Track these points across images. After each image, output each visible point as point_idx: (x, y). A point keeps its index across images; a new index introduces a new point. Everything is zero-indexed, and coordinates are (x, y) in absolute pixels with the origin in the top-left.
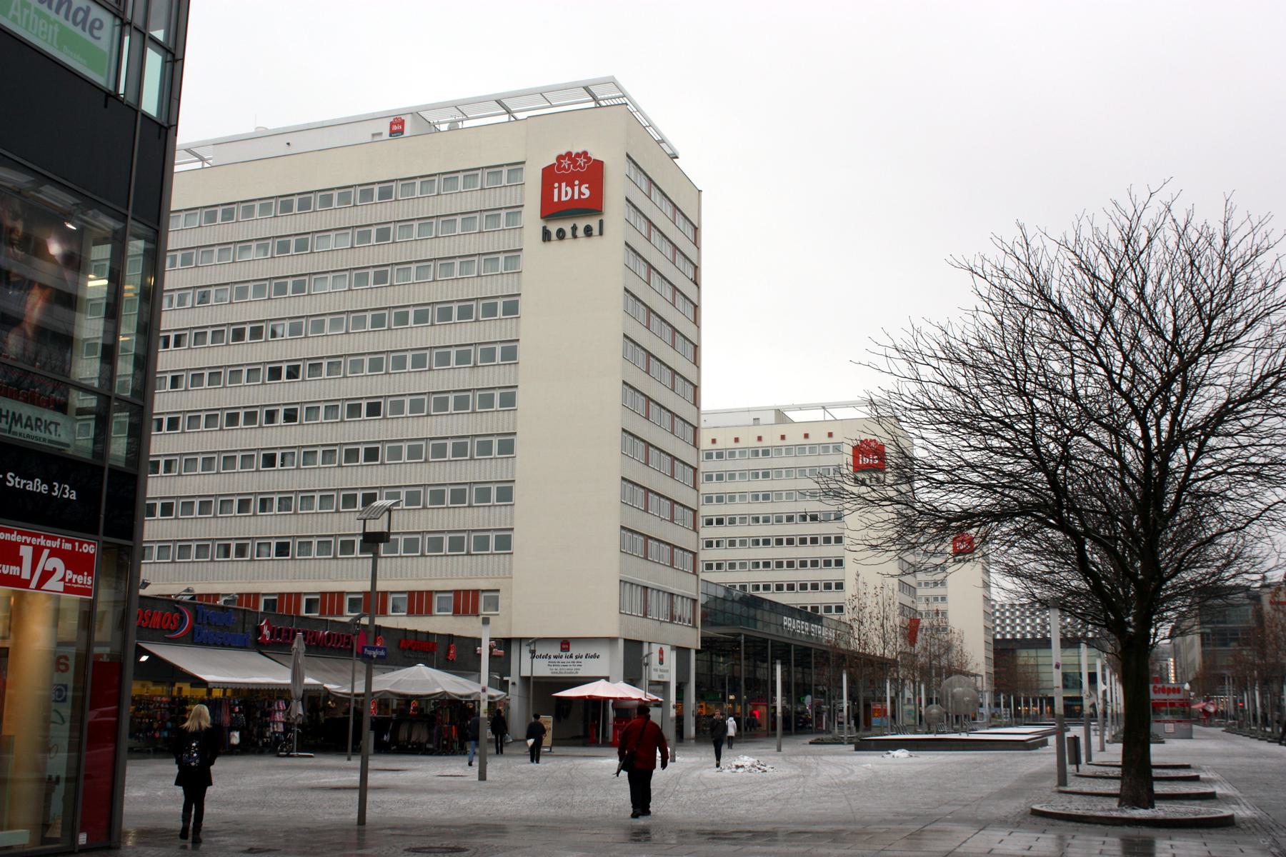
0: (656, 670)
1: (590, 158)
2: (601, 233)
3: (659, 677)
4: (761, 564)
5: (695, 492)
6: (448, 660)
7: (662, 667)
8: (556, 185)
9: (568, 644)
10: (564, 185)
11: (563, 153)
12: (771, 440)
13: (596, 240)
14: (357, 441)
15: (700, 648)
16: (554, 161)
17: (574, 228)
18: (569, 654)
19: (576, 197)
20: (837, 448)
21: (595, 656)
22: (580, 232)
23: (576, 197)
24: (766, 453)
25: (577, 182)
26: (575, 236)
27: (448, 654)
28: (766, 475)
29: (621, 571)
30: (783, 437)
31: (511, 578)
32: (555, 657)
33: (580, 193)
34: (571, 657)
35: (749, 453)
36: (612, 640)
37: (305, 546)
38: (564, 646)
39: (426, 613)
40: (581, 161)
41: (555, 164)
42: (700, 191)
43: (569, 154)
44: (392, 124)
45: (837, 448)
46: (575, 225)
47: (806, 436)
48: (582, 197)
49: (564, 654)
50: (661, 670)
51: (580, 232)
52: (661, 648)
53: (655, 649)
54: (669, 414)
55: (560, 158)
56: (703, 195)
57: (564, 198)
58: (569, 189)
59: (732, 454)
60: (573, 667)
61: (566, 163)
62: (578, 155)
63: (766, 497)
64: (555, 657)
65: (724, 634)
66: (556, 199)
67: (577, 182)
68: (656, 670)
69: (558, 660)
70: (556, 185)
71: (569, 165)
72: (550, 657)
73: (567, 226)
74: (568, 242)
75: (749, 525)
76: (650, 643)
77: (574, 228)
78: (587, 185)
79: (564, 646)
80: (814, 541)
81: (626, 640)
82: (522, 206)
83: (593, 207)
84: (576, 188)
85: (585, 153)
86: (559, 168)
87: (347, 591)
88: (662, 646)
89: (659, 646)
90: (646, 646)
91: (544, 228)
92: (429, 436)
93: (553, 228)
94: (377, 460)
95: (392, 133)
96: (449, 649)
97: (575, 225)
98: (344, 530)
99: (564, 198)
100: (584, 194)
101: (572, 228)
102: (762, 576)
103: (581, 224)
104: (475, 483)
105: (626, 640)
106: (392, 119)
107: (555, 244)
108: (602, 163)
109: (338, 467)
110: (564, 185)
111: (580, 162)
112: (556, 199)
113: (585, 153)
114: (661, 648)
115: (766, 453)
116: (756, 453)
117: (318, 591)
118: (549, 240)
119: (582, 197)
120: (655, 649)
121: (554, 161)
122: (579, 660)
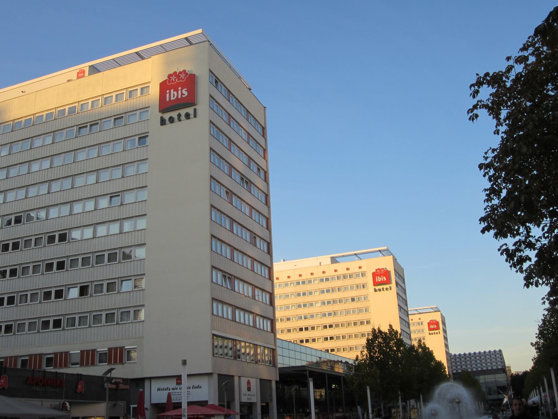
0: (245, 395)
1: (187, 74)
2: (195, 116)
3: (248, 399)
5: (270, 282)
6: (77, 392)
7: (249, 393)
8: (168, 91)
10: (172, 91)
11: (172, 73)
12: (330, 273)
13: (192, 120)
14: (52, 258)
15: (278, 380)
17: (179, 115)
19: (180, 97)
21: (199, 387)
23: (180, 97)
24: (327, 280)
25: (180, 88)
26: (180, 120)
27: (76, 388)
29: (213, 328)
30: (336, 271)
32: (173, 389)
36: (210, 374)
37: (21, 327)
38: (178, 381)
39: (91, 365)
41: (167, 79)
42: (265, 107)
43: (175, 73)
44: (78, 73)
46: (179, 113)
49: (178, 387)
50: (249, 395)
51: (183, 117)
52: (249, 380)
53: (244, 381)
54: (249, 232)
56: (267, 109)
57: (172, 98)
58: (175, 93)
59: (310, 282)
61: (173, 78)
62: (180, 73)
64: (173, 389)
65: (296, 371)
66: (168, 99)
67: (180, 88)
68: (245, 395)
69: (175, 391)
70: (168, 91)
71: (175, 79)
72: (170, 390)
73: (174, 114)
74: (176, 124)
76: (239, 377)
77: (179, 115)
78: (186, 89)
79: (178, 381)
81: (219, 375)
83: (190, 101)
84: (180, 92)
85: (184, 71)
86: (169, 82)
87: (45, 353)
88: (249, 379)
89: (246, 379)
90: (236, 379)
91: (162, 118)
92: (94, 251)
93: (167, 116)
94: (64, 269)
95: (78, 78)
96: (77, 385)
97: (179, 113)
98: (44, 314)
99: (172, 98)
100: (184, 95)
101: (178, 115)
102: (329, 345)
103: (183, 112)
104: (121, 277)
105: (219, 375)
106: (78, 71)
107: (169, 126)
108: (194, 75)
109: (41, 275)
110: (172, 91)
111: (181, 76)
112: (168, 99)
113: (184, 71)
114: (249, 380)
115: (327, 280)
116: (322, 280)
117: (28, 354)
118: (165, 124)
120: (244, 381)
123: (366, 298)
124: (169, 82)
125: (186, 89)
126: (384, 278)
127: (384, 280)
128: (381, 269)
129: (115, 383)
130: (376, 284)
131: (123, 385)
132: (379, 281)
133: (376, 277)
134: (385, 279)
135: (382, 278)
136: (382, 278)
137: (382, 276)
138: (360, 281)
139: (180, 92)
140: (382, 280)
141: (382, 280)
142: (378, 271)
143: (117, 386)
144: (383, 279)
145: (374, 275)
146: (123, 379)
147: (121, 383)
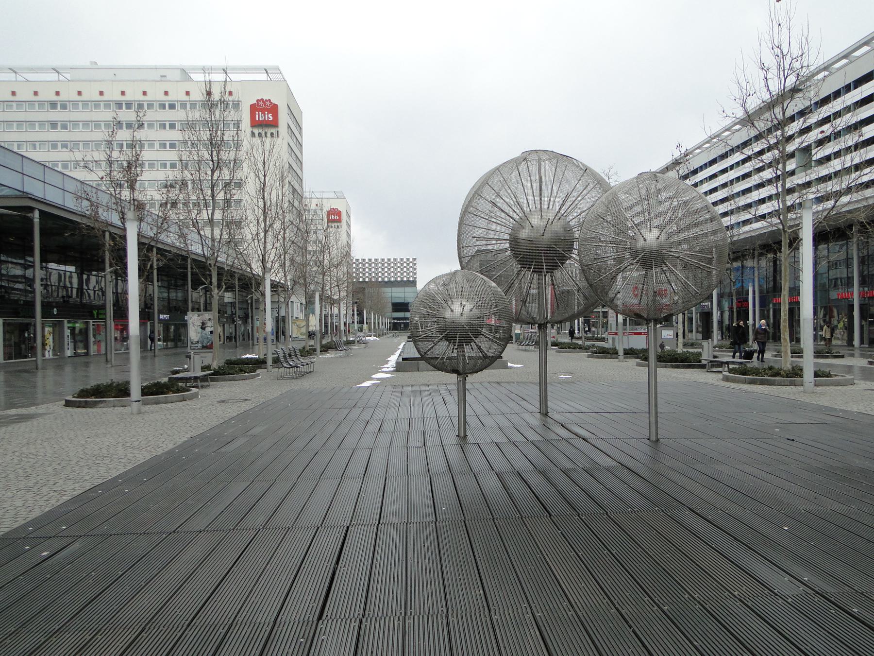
1: (272, 103)
16: (255, 102)
17: (266, 133)
22: (269, 135)
40: (268, 103)
43: (262, 99)
51: (269, 135)
55: (258, 101)
57: (261, 119)
61: (261, 103)
62: (266, 100)
66: (257, 119)
83: (274, 124)
84: (266, 115)
86: (258, 105)
91: (252, 132)
93: (256, 131)
99: (261, 119)
110: (260, 113)
113: (270, 100)
124: (258, 105)
126: (270, 115)
133: (257, 113)
135: (266, 115)
137: (266, 113)
140: (267, 119)
141: (267, 119)
145: (254, 108)
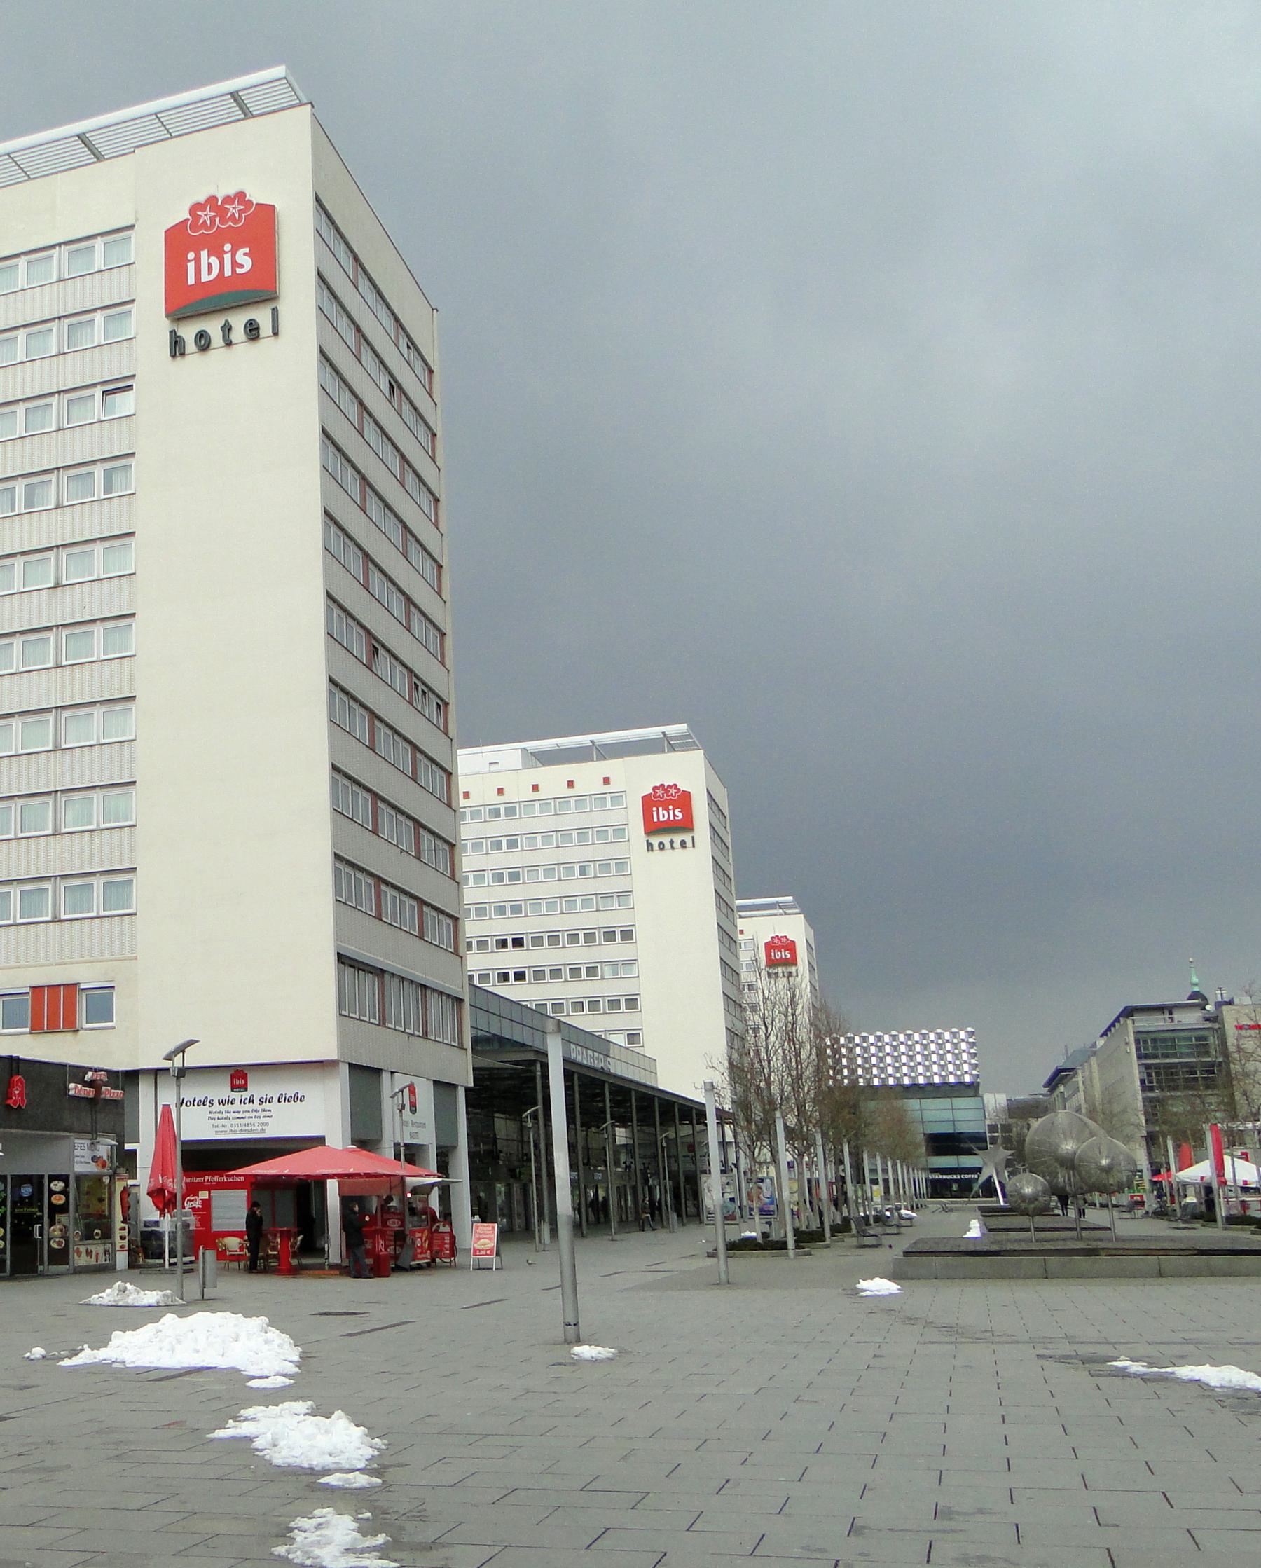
2: (276, 334)
4: (512, 977)
8: (191, 255)
9: (245, 1077)
10: (204, 254)
16: (185, 215)
17: (227, 329)
18: (246, 1095)
19: (228, 273)
20: (617, 797)
21: (297, 1098)
22: (238, 334)
23: (228, 273)
24: (511, 812)
25: (228, 247)
27: (8, 1095)
28: (512, 844)
31: (136, 958)
32: (222, 1102)
33: (235, 264)
34: (251, 1101)
35: (485, 812)
38: (237, 1082)
40: (234, 209)
41: (188, 219)
45: (617, 797)
47: (571, 784)
48: (239, 271)
49: (237, 1096)
51: (238, 334)
55: (195, 208)
57: (205, 277)
58: (214, 261)
60: (256, 1121)
61: (206, 216)
62: (228, 200)
63: (514, 876)
64: (222, 1102)
66: (191, 281)
67: (228, 247)
70: (191, 255)
72: (211, 1103)
74: (217, 353)
75: (491, 918)
77: (227, 329)
78: (247, 250)
79: (237, 1082)
80: (590, 937)
81: (351, 1065)
82: (132, 301)
84: (228, 257)
85: (241, 195)
86: (195, 226)
96: (10, 1086)
99: (205, 277)
100: (242, 266)
105: (351, 1065)
107: (193, 359)
110: (204, 254)
112: (191, 281)
113: (241, 195)
115: (511, 812)
116: (496, 813)
118: (183, 354)
119: (239, 271)
121: (185, 215)
122: (266, 1106)
123: (622, 864)
124: (195, 226)
125: (247, 250)
126: (677, 812)
127: (676, 818)
128: (669, 787)
129: (91, 1084)
130: (652, 828)
131: (109, 1088)
132: (661, 819)
133: (654, 809)
134: (680, 816)
135: (671, 812)
136: (671, 812)
137: (671, 807)
138: (611, 817)
139: (228, 257)
140: (672, 818)
141: (672, 818)
142: (660, 792)
143: (98, 1092)
144: (674, 815)
145: (648, 803)
146: (112, 1074)
147: (106, 1084)
